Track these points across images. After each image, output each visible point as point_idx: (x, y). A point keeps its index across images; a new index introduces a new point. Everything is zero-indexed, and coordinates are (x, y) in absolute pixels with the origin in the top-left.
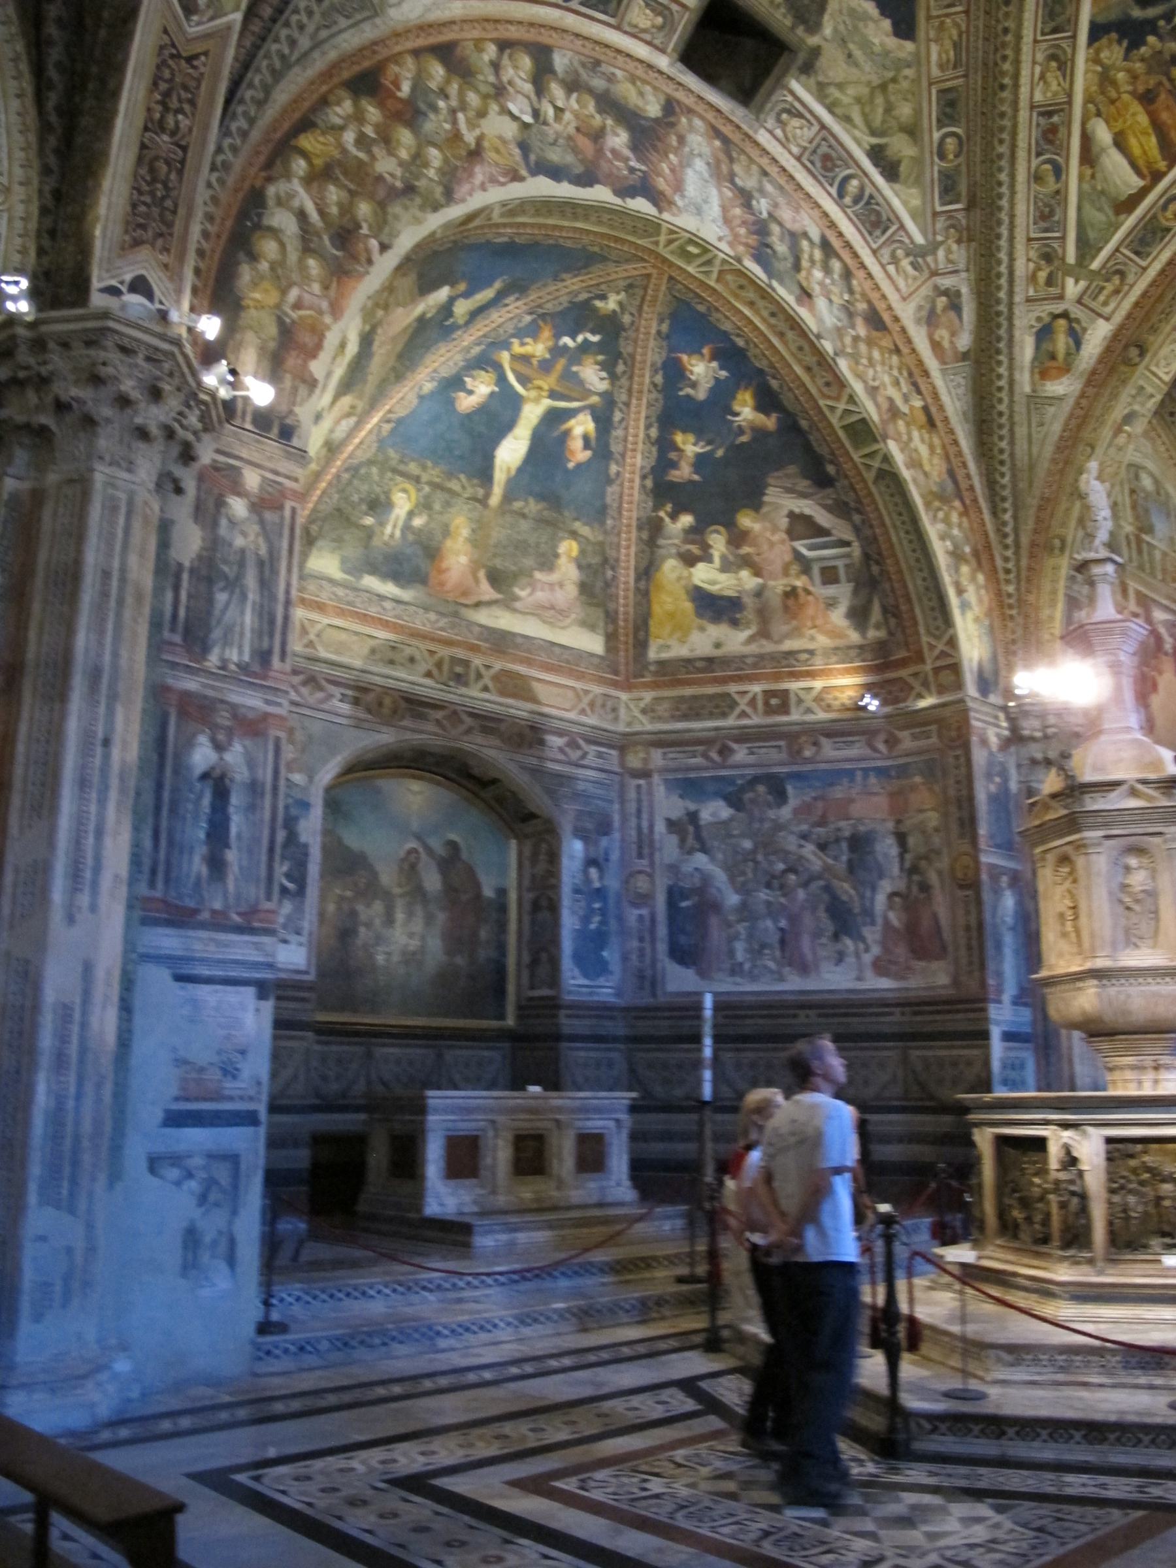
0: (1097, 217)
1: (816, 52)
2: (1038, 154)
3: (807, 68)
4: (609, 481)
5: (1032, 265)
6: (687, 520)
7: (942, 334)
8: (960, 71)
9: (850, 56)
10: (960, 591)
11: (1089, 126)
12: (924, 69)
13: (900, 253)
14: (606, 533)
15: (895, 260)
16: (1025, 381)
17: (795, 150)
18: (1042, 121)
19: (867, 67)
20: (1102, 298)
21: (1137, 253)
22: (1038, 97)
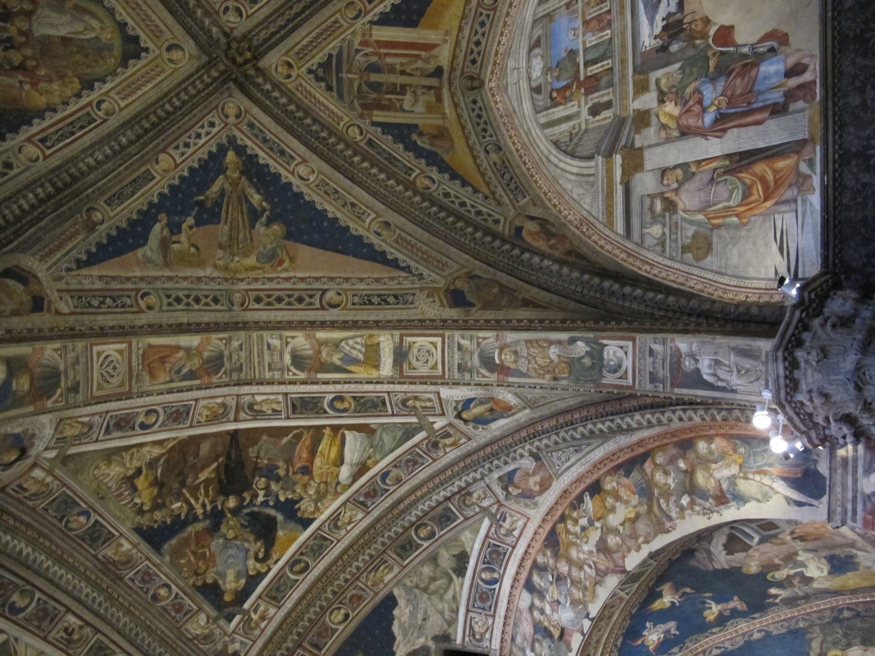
0: (388, 439)
1: (436, 638)
2: (387, 490)
3: (445, 638)
4: (768, 635)
5: (448, 450)
6: (773, 591)
7: (533, 482)
8: (385, 557)
9: (424, 619)
10: (721, 499)
11: (349, 482)
12: (400, 576)
13: (503, 531)
14: (811, 626)
15: (509, 533)
16: (524, 415)
17: (490, 621)
18: (369, 503)
19: (423, 605)
20: (429, 404)
21: (384, 403)
22: (360, 515)
